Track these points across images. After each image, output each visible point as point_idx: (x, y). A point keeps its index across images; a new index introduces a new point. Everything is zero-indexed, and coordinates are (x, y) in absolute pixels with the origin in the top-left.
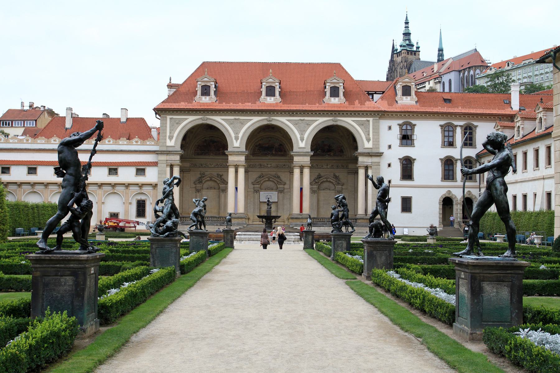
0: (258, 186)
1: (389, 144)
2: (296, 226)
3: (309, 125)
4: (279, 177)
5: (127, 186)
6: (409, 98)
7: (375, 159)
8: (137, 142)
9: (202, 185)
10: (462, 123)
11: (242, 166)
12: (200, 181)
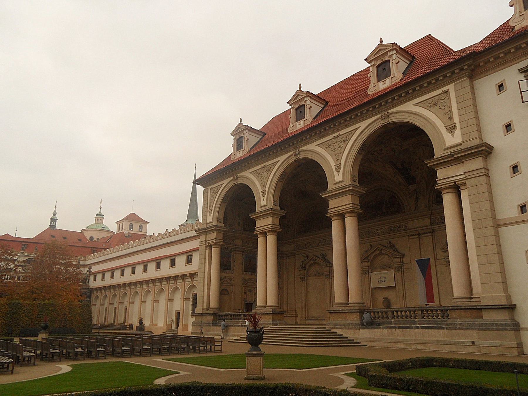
2: (335, 328)
3: (346, 141)
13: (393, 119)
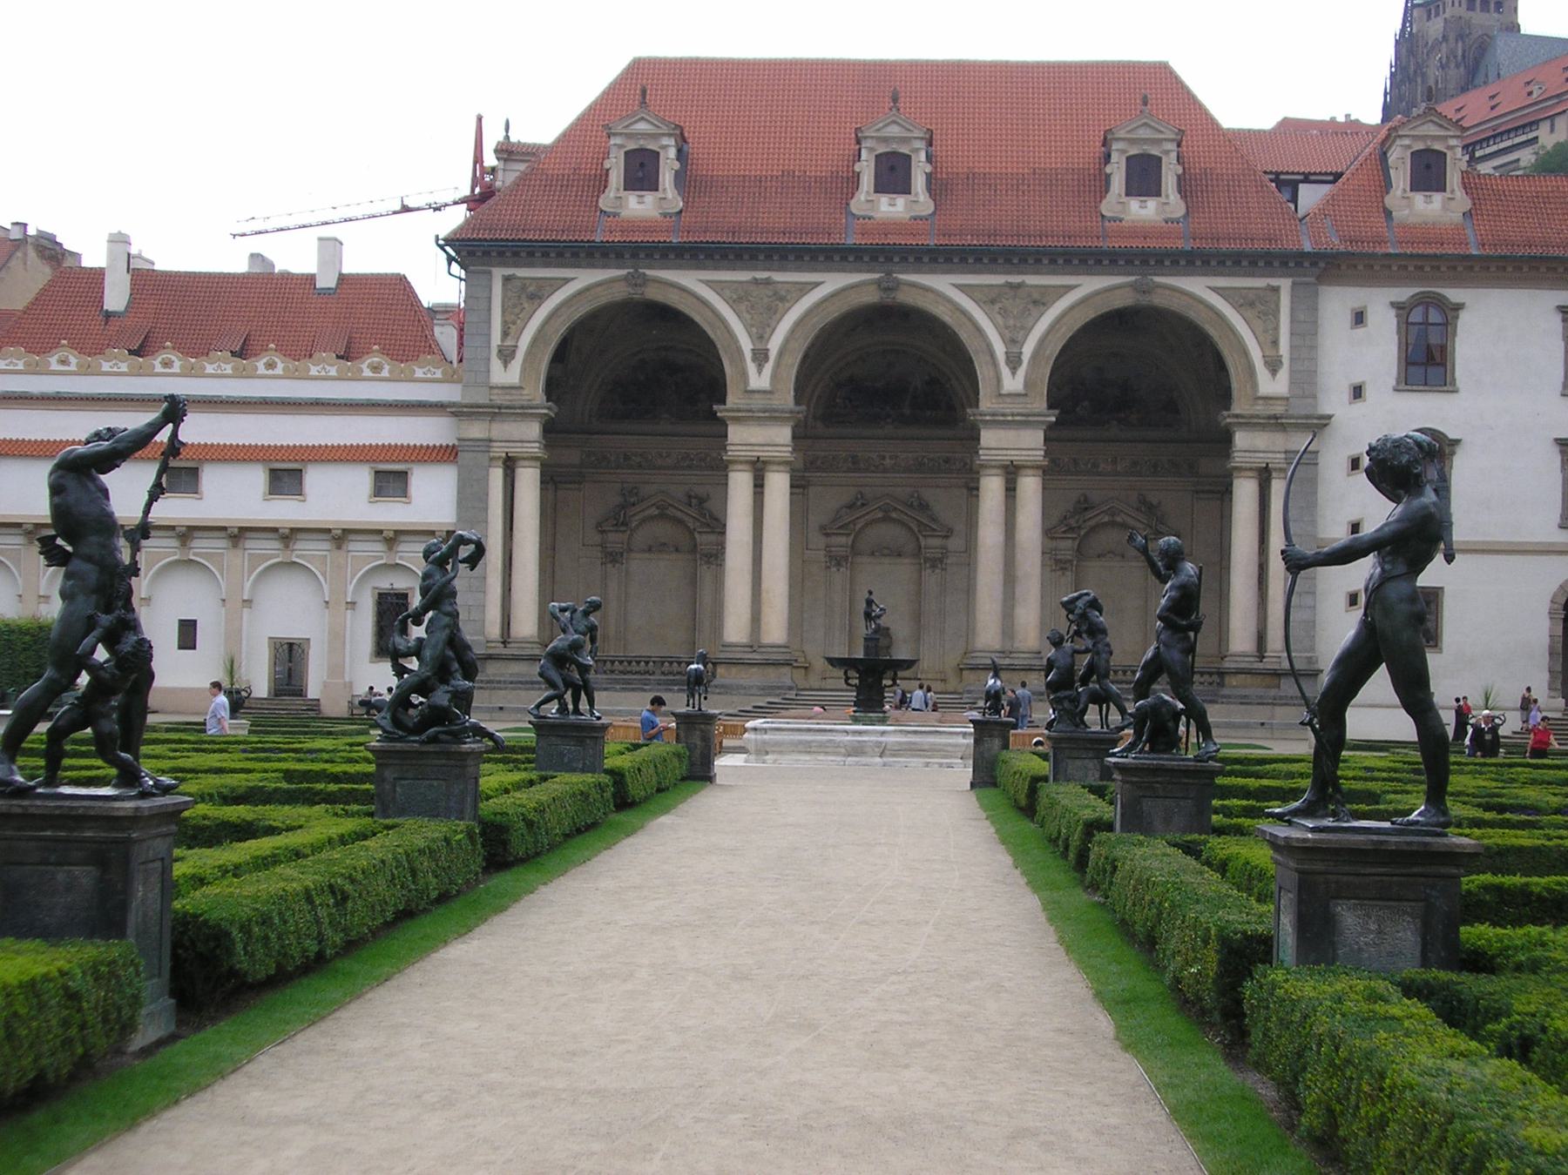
0: (842, 540)
1: (1357, 380)
4: (924, 507)
5: (341, 537)
6: (1437, 198)
7: (1300, 442)
8: (376, 368)
9: (626, 536)
11: (779, 463)
12: (618, 519)
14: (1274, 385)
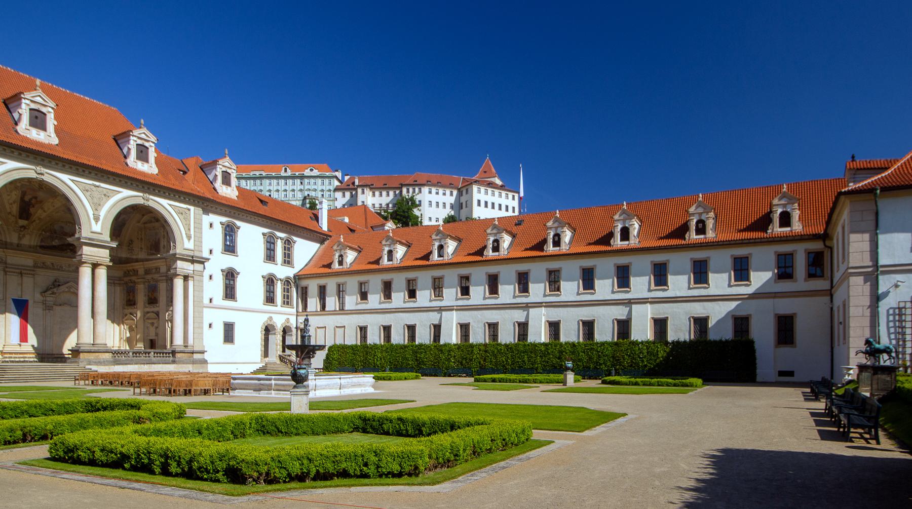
7: (198, 267)
10: (282, 235)
13: (151, 204)
14: (189, 245)
